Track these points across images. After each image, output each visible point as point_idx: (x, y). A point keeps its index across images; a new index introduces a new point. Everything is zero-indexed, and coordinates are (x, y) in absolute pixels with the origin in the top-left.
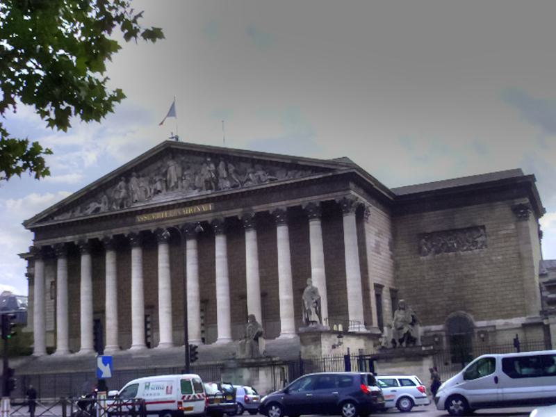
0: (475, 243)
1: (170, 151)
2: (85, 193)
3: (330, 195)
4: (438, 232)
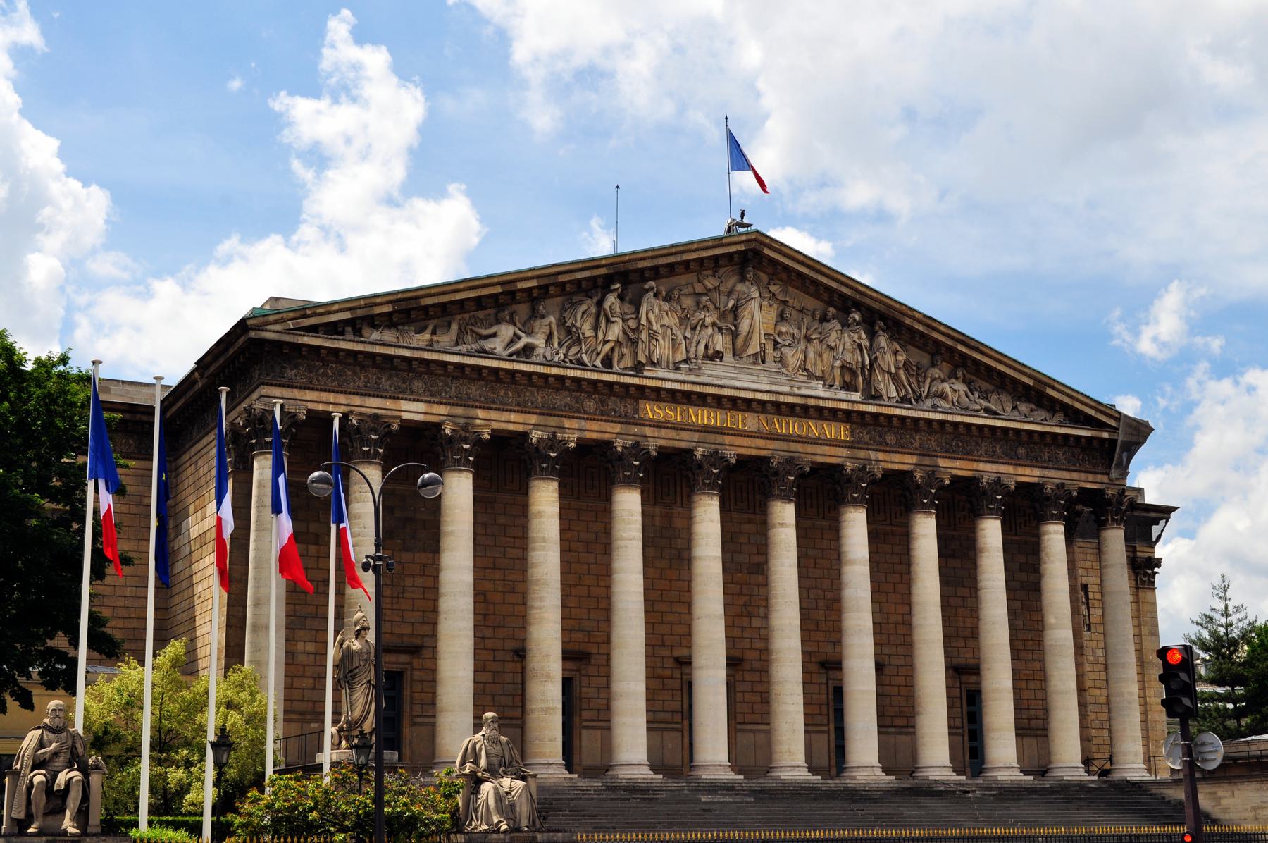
1: (750, 258)
2: (498, 289)
3: (1091, 477)
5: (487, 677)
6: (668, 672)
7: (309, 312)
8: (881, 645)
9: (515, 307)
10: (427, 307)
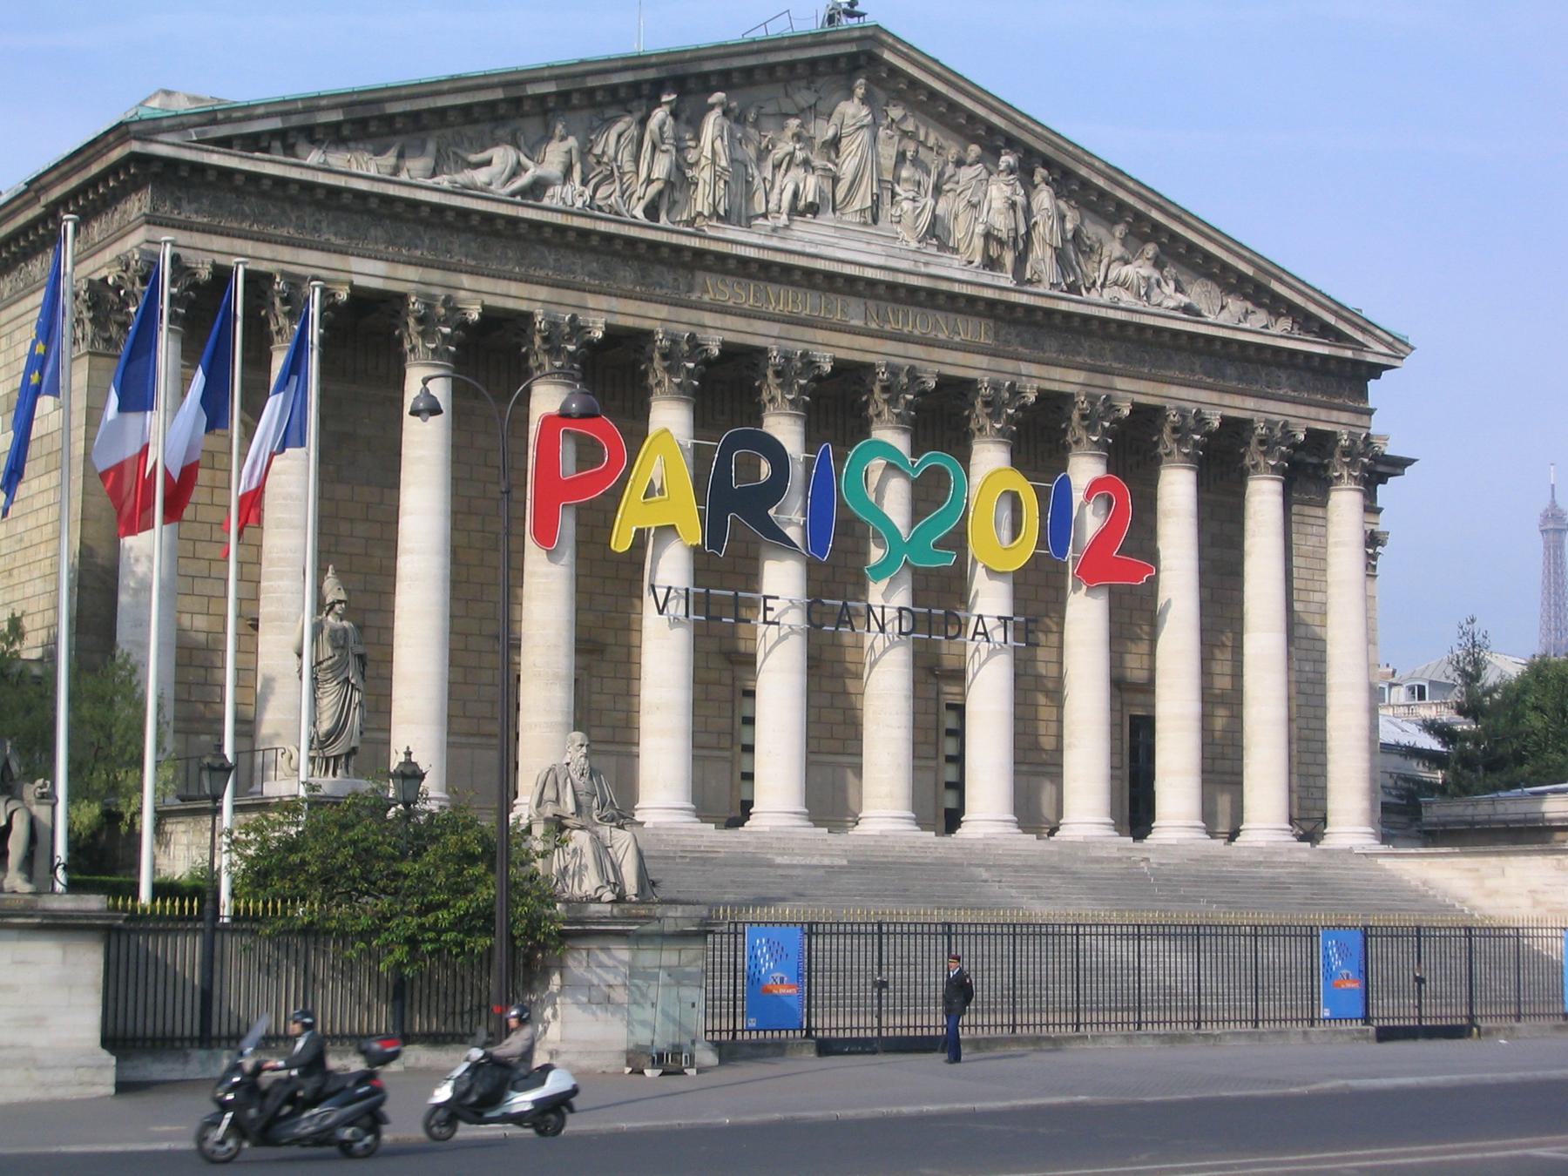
2: (499, 94)
3: (1323, 414)
7: (220, 116)
10: (392, 117)
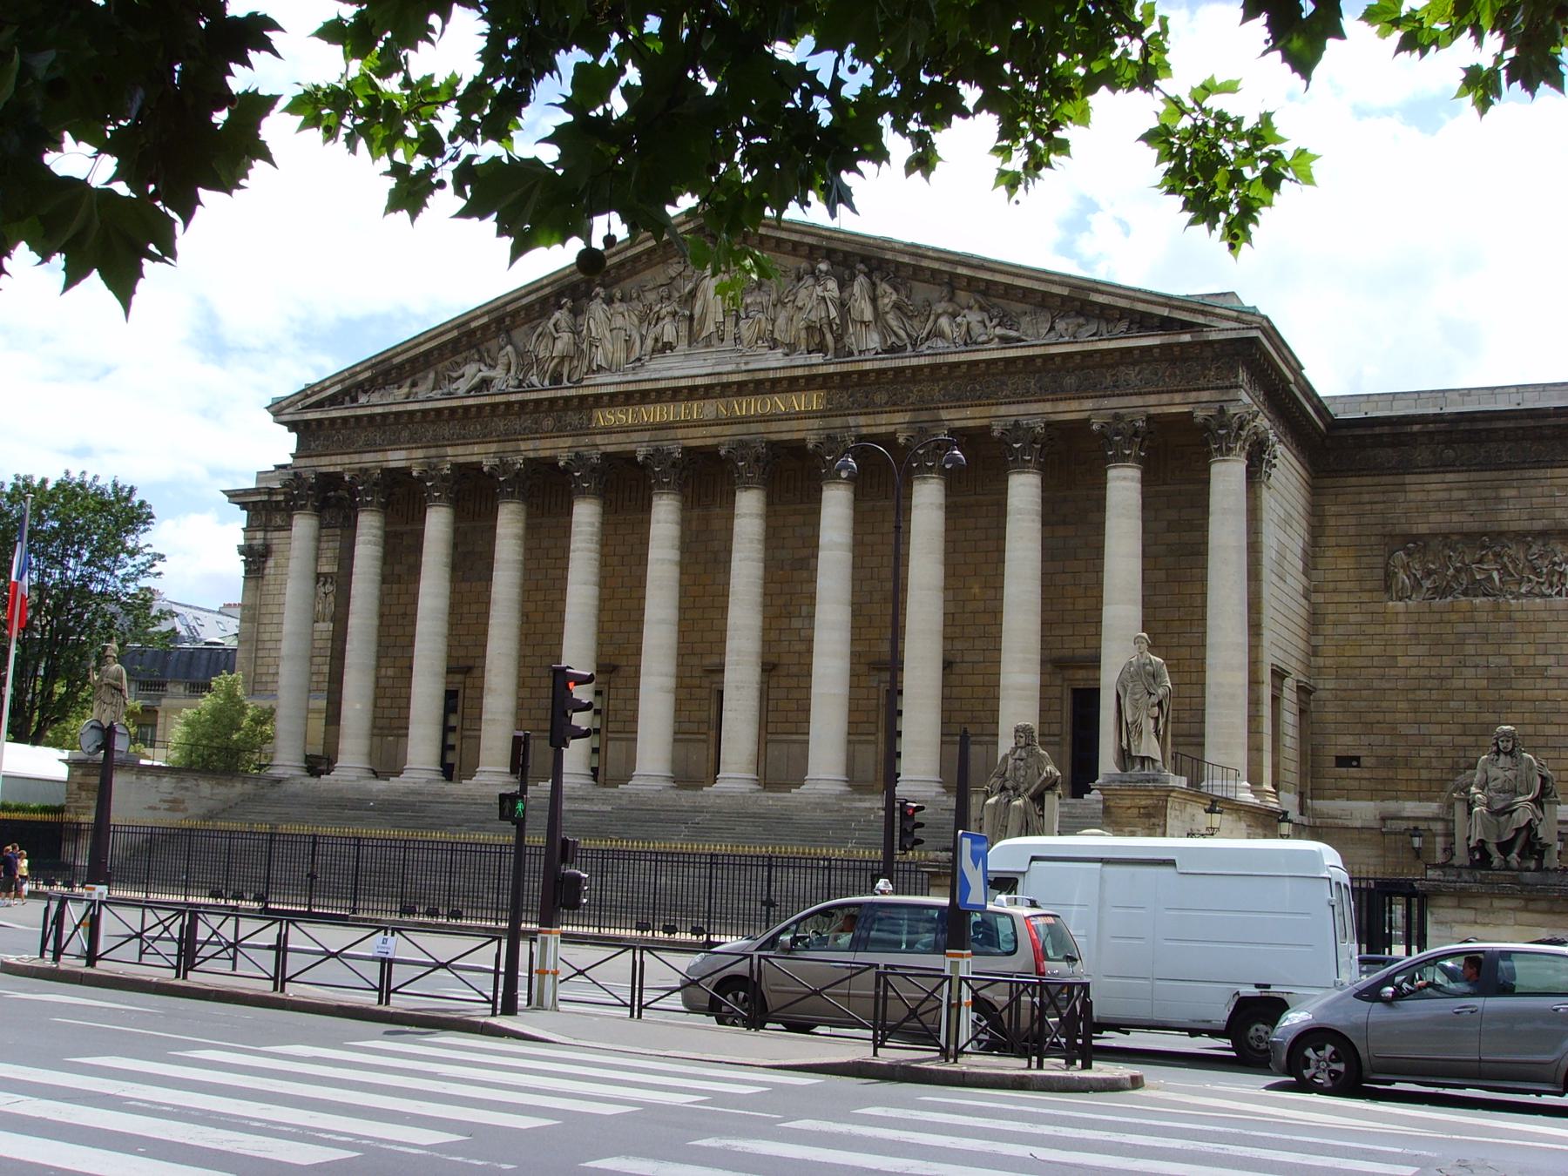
0: (1555, 578)
2: (455, 333)
3: (1178, 398)
4: (1446, 536)
5: (526, 692)
6: (697, 682)
8: (952, 639)
9: (487, 345)
10: (401, 365)
